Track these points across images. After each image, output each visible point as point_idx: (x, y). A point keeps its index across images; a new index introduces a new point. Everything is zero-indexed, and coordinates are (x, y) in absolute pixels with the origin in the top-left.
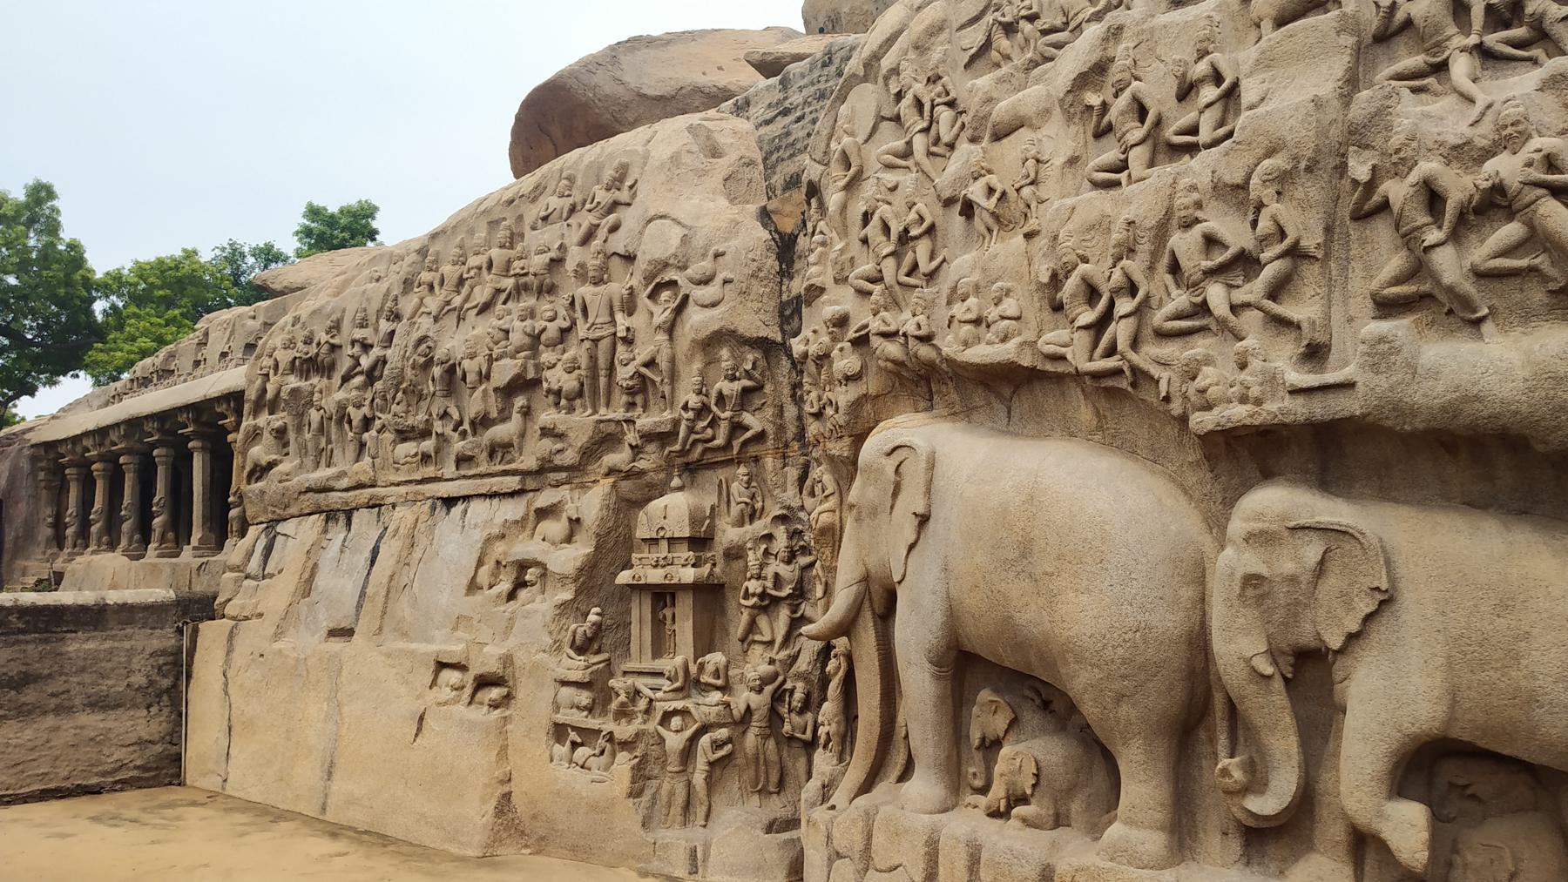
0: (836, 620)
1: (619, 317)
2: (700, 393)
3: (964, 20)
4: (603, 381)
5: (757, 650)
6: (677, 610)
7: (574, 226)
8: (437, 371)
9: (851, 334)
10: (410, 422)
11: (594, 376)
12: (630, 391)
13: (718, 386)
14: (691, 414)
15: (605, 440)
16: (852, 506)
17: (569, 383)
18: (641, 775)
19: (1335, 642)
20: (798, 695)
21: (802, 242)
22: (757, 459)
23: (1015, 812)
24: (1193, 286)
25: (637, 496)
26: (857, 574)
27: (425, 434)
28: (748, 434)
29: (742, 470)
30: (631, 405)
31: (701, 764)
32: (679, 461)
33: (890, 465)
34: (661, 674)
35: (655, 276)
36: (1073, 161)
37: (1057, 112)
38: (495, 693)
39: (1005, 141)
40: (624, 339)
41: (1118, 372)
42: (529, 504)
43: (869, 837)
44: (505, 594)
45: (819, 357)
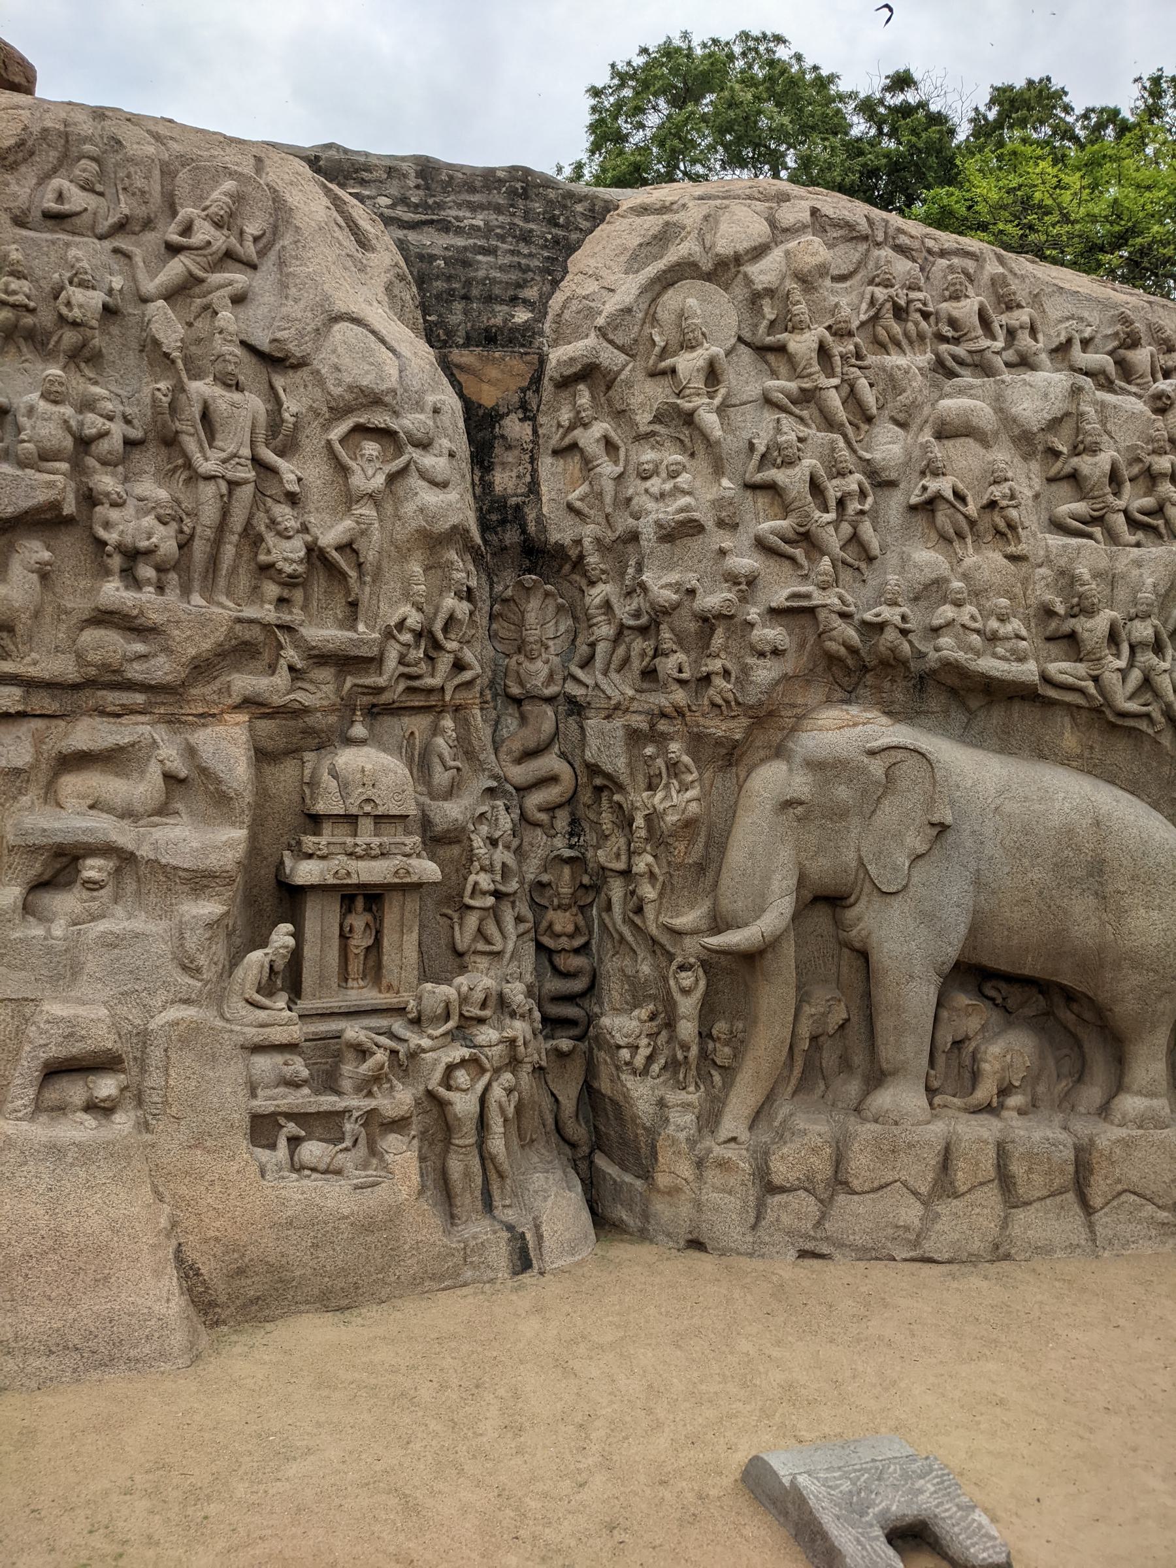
2: (420, 610)
3: (836, 272)
4: (229, 551)
6: (391, 918)
11: (217, 543)
12: (292, 581)
14: (407, 637)
15: (241, 651)
16: (788, 804)
18: (422, 1159)
20: (537, 1015)
21: (515, 428)
23: (1015, 1100)
25: (281, 743)
26: (792, 882)
28: (467, 675)
29: (448, 723)
30: (282, 601)
31: (497, 1125)
32: (367, 700)
33: (877, 767)
34: (401, 1011)
35: (348, 411)
36: (1037, 496)
37: (1004, 437)
38: (106, 1086)
39: (945, 442)
40: (292, 499)
41: (1147, 716)
42: (38, 741)
44: (20, 904)
45: (720, 616)
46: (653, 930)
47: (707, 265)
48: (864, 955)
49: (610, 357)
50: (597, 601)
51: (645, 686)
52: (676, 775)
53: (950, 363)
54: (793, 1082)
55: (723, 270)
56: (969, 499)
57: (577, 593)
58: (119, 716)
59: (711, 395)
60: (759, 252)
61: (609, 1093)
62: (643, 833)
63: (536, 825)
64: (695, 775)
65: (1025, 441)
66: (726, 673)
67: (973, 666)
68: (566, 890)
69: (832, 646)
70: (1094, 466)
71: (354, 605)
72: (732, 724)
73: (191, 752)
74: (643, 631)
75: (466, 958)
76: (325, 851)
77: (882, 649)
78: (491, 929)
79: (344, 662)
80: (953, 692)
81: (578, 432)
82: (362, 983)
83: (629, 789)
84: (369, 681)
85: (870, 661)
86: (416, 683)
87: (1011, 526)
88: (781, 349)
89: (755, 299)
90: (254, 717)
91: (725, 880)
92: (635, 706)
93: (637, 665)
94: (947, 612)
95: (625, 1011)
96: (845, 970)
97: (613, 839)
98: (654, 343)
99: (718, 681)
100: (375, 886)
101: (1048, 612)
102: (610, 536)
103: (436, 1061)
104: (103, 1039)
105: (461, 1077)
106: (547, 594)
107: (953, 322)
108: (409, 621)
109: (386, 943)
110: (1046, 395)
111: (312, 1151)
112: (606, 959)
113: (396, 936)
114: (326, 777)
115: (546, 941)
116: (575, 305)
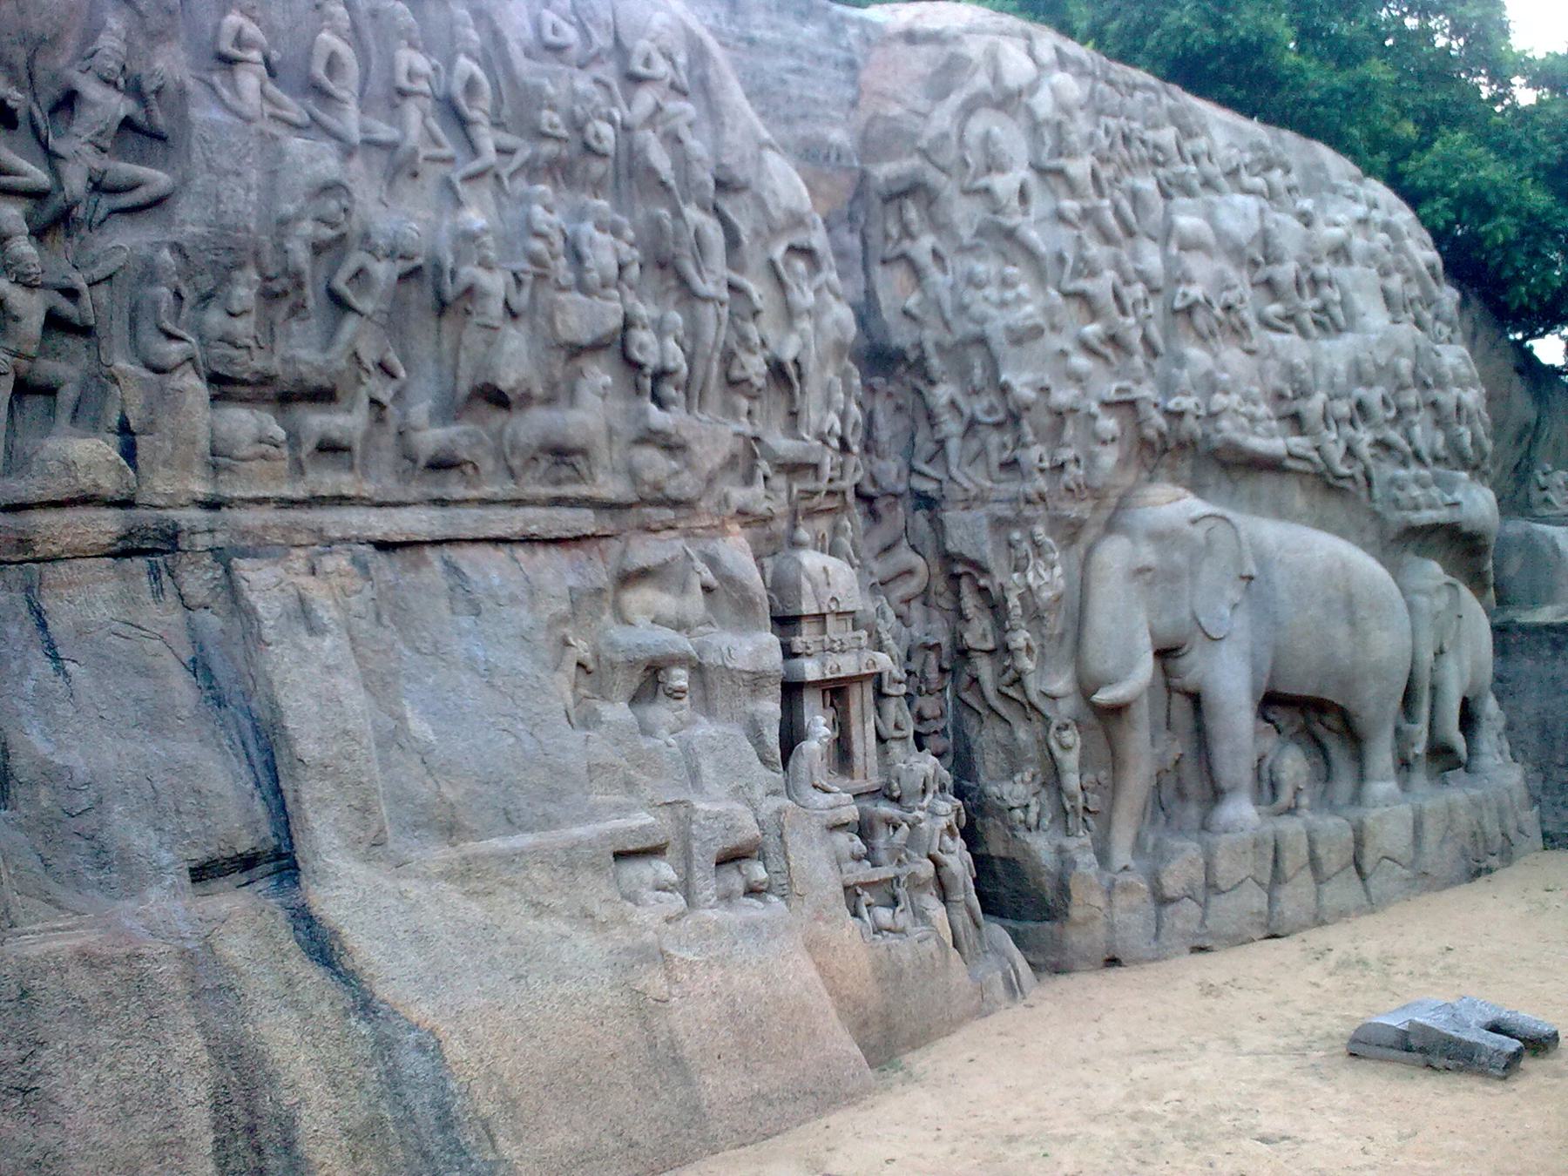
1: (736, 278)
6: (854, 710)
7: (616, 88)
8: (384, 271)
9: (1112, 396)
10: (258, 364)
11: (709, 360)
14: (835, 443)
16: (1141, 571)
17: (676, 358)
19: (1446, 647)
24: (1376, 427)
26: (1147, 640)
27: (323, 396)
30: (749, 413)
32: (804, 505)
35: (783, 230)
38: (758, 872)
40: (756, 313)
41: (1352, 477)
43: (1209, 867)
45: (1073, 411)
46: (1035, 698)
47: (997, 97)
48: (1196, 699)
49: (933, 176)
50: (944, 400)
51: (1003, 476)
52: (1040, 555)
53: (1164, 183)
54: (1148, 816)
55: (1008, 101)
56: (1215, 303)
57: (911, 397)
58: (656, 531)
59: (1026, 213)
60: (1033, 88)
61: (1003, 853)
62: (1019, 611)
65: (1236, 252)
68: (933, 675)
69: (1150, 433)
70: (1286, 272)
72: (1083, 505)
73: (712, 562)
74: (998, 426)
79: (793, 468)
80: (1226, 466)
81: (906, 245)
84: (810, 485)
85: (1172, 444)
87: (1245, 325)
88: (1060, 173)
89: (1035, 127)
90: (744, 525)
92: (993, 496)
93: (995, 458)
94: (1220, 400)
95: (1002, 779)
96: (1175, 713)
97: (976, 621)
98: (967, 165)
99: (1071, 468)
101: (1281, 396)
102: (948, 339)
103: (933, 830)
104: (749, 829)
105: (946, 838)
106: (890, 395)
107: (1157, 147)
110: (1245, 216)
111: (884, 915)
112: (973, 735)
114: (803, 579)
116: (880, 125)
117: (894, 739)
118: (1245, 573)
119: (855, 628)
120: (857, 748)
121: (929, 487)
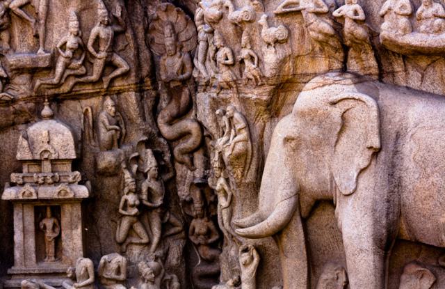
0: (279, 223)
2: (77, 35)
5: (136, 250)
9: (279, 9)
13: (94, 31)
14: (68, 53)
22: (119, 93)
26: (289, 191)
28: (118, 72)
29: (109, 102)
33: (336, 112)
45: (242, 22)
51: (217, 70)
62: (217, 164)
63: (182, 163)
64: (241, 124)
66: (252, 58)
67: (400, 40)
68: (197, 205)
71: (37, 36)
72: (260, 90)
75: (124, 247)
76: (21, 181)
77: (346, 33)
78: (139, 229)
79: (33, 71)
82: (53, 258)
83: (216, 136)
84: (48, 82)
86: (82, 80)
91: (261, 194)
99: (247, 63)
100: (52, 200)
108: (69, 45)
109: (63, 235)
113: (68, 231)
114: (21, 138)
115: (192, 238)
117: (136, 244)
118: (369, 144)
119: (73, 170)
120: (66, 244)
121: (195, 75)
